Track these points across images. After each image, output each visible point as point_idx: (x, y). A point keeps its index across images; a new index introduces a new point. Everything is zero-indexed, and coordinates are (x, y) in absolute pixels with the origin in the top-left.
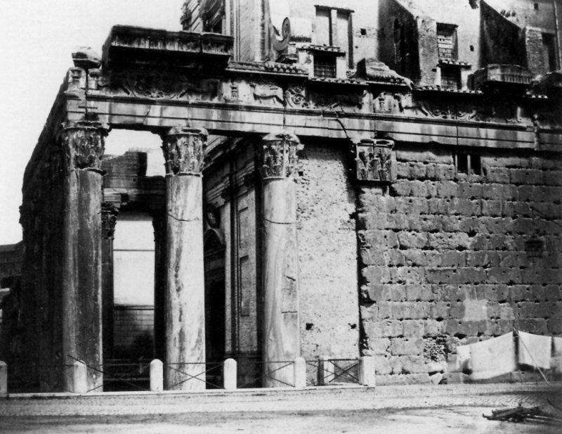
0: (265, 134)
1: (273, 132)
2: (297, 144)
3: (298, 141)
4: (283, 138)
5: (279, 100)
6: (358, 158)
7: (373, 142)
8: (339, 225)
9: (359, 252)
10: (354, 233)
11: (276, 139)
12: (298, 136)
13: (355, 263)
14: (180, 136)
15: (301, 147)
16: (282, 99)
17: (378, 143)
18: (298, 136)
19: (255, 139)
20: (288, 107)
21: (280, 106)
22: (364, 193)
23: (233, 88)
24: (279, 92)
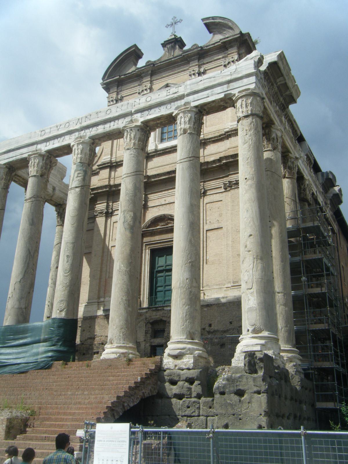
0: (291, 153)
24: (292, 135)
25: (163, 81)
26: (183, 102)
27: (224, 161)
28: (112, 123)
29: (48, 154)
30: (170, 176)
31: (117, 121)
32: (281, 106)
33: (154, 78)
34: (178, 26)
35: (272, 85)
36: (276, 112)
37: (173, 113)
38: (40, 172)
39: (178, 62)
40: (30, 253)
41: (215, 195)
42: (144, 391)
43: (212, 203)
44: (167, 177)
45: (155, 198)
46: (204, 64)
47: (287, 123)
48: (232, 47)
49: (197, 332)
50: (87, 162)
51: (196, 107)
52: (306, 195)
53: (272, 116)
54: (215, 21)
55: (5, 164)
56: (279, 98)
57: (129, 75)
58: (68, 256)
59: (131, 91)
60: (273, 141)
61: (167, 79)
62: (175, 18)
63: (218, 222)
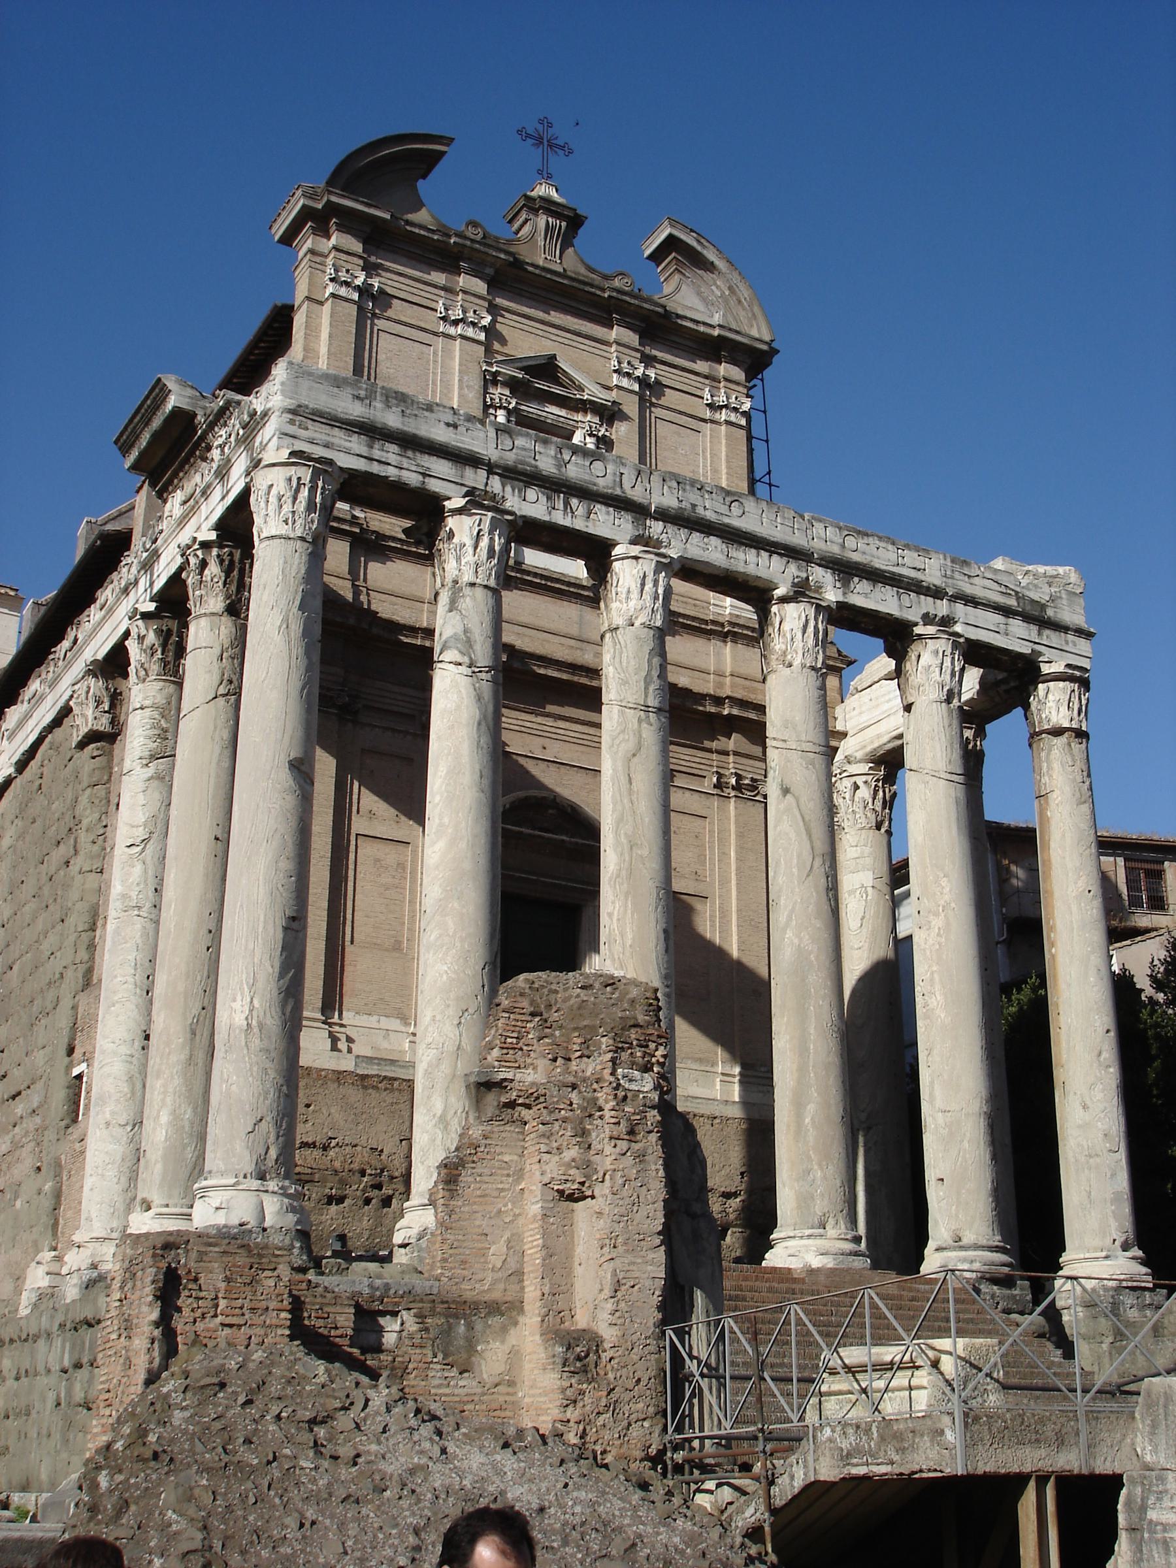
25: (526, 328)
26: (942, 608)
27: (735, 712)
28: (751, 555)
30: (576, 679)
31: (764, 554)
34: (557, 161)
37: (916, 624)
41: (688, 793)
43: (681, 816)
44: (565, 676)
45: (512, 727)
54: (705, 252)
57: (422, 232)
59: (415, 291)
61: (540, 333)
62: (550, 125)
63: (694, 877)
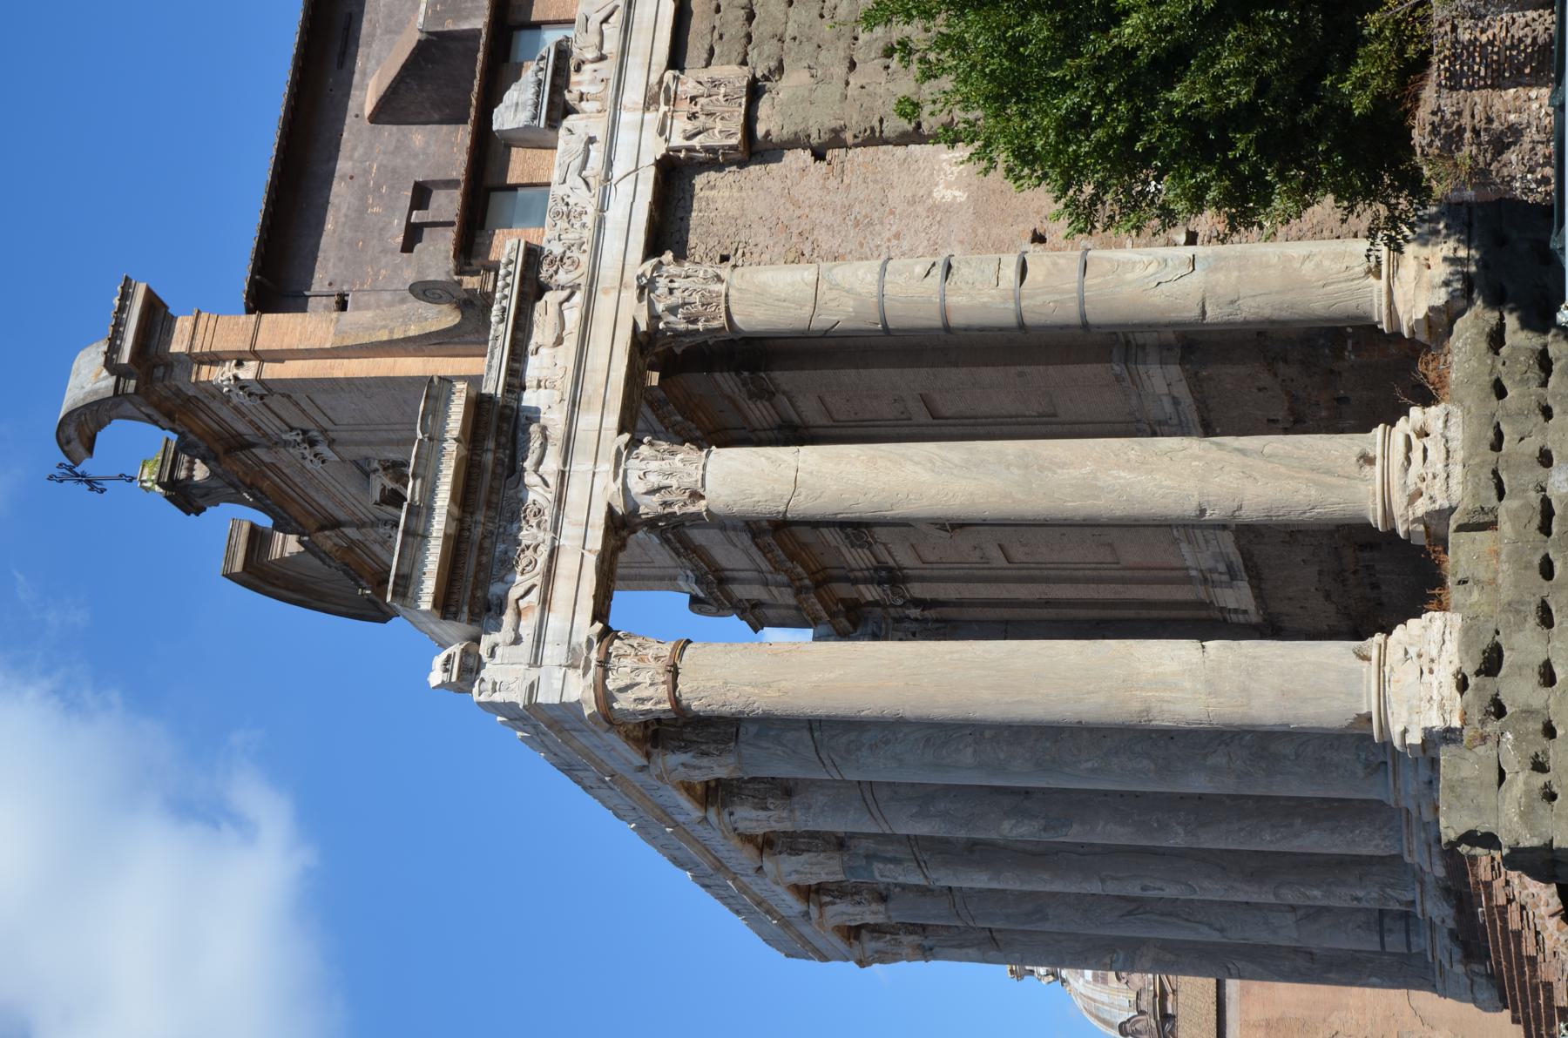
0: (635, 325)
1: (634, 312)
2: (660, 262)
3: (654, 261)
4: (645, 288)
5: (568, 299)
6: (696, 142)
7: (665, 114)
8: (833, 183)
9: (886, 142)
10: (851, 152)
11: (645, 303)
12: (644, 260)
13: (914, 148)
14: (625, 489)
15: (668, 256)
16: (566, 293)
17: (667, 102)
18: (644, 260)
19: (649, 347)
20: (583, 281)
21: (579, 298)
22: (768, 133)
23: (539, 386)
29: (812, 895)
32: (503, 440)
33: (342, 515)
35: (481, 548)
36: (560, 500)
38: (874, 907)
39: (273, 482)
40: (1130, 913)
42: (1543, 910)
46: (265, 435)
47: (534, 368)
48: (178, 392)
49: (1363, 756)
50: (837, 855)
51: (648, 756)
52: (731, 147)
53: (596, 541)
55: (851, 945)
56: (494, 472)
58: (1144, 889)
60: (671, 504)
